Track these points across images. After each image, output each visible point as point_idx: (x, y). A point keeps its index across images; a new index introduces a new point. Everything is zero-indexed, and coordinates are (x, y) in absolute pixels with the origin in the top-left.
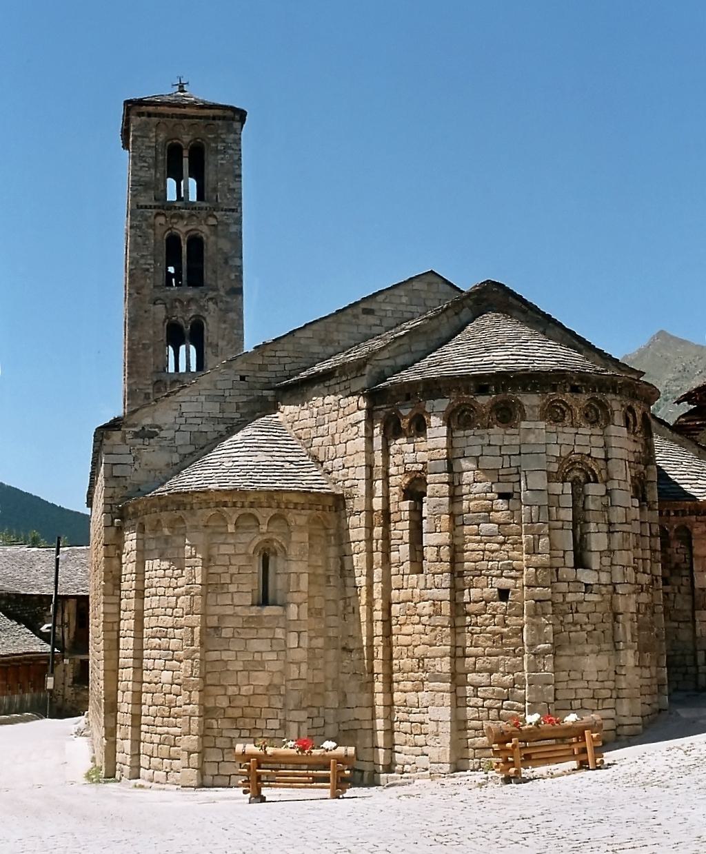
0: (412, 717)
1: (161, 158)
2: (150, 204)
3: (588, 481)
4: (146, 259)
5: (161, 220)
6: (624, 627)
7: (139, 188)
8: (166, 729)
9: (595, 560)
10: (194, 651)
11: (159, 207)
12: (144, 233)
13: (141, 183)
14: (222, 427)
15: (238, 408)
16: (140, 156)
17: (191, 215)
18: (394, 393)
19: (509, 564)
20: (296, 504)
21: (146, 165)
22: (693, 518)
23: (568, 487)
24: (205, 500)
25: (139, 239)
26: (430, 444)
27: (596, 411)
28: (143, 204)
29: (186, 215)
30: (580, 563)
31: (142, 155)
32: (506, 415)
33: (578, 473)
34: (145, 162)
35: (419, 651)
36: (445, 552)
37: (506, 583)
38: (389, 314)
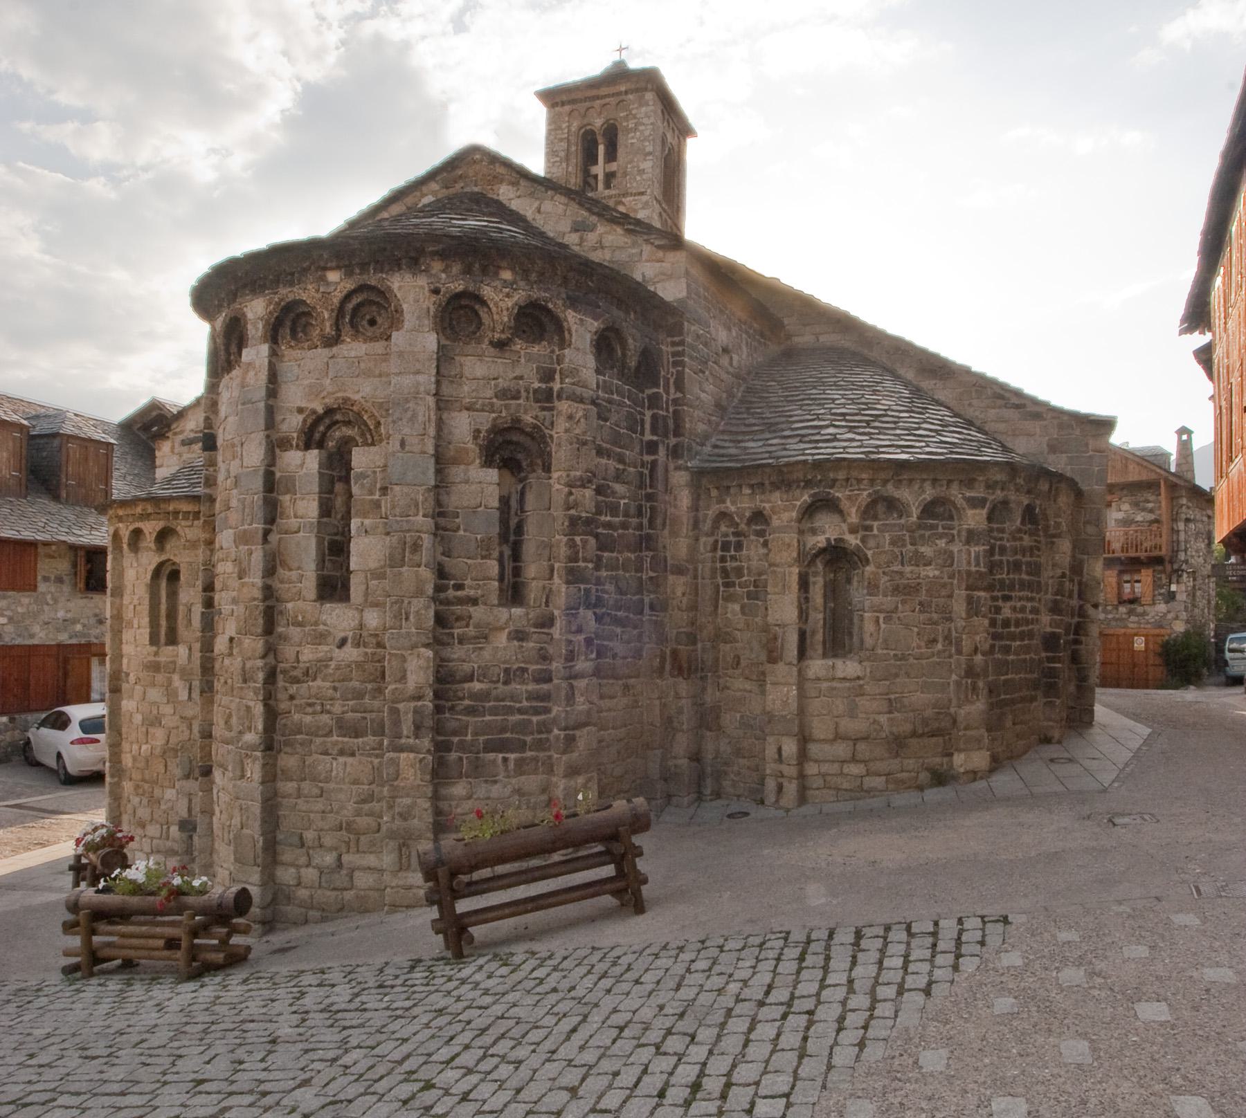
1: (573, 148)
6: (395, 712)
22: (777, 498)
23: (312, 459)
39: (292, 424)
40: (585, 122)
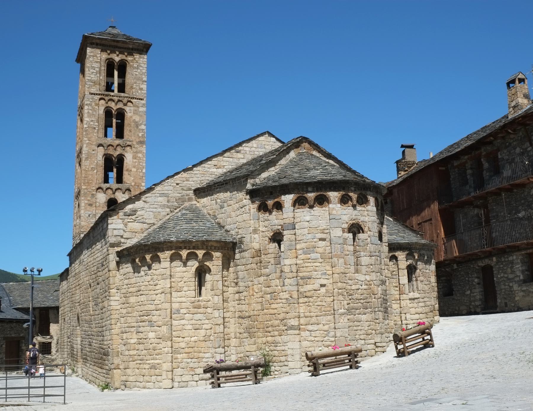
0: (278, 348)
1: (103, 68)
3: (359, 233)
4: (94, 123)
5: (102, 102)
7: (91, 83)
8: (153, 361)
9: (364, 269)
10: (167, 321)
11: (101, 95)
14: (168, 210)
15: (176, 200)
17: (119, 101)
18: (263, 192)
19: (326, 273)
20: (215, 247)
21: (95, 71)
24: (170, 246)
25: (90, 111)
26: (285, 216)
27: (362, 199)
28: (92, 92)
29: (116, 100)
30: (357, 271)
32: (322, 200)
33: (355, 229)
34: (94, 69)
35: (281, 316)
36: (294, 269)
37: (324, 282)
38: (248, 152)
39: (346, 226)
40: (110, 57)
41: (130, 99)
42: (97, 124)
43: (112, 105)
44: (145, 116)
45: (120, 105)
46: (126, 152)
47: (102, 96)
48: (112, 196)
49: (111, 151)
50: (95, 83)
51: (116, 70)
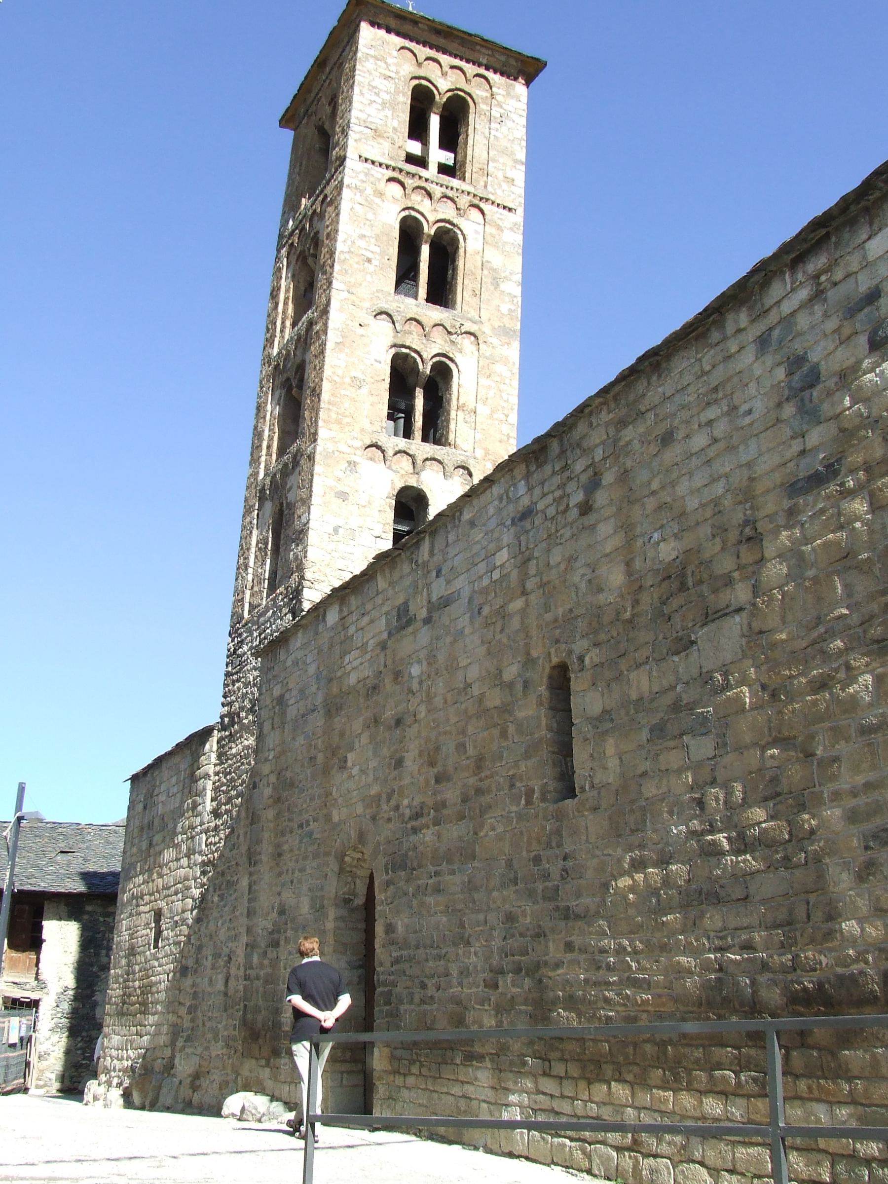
2: (382, 161)
11: (394, 169)
12: (366, 200)
13: (367, 125)
16: (369, 85)
25: (358, 208)
31: (373, 84)
34: (377, 94)
41: (476, 201)
42: (377, 250)
43: (424, 205)
44: (520, 259)
45: (447, 211)
46: (460, 351)
47: (395, 174)
48: (412, 482)
49: (414, 340)
50: (377, 133)
51: (438, 119)
